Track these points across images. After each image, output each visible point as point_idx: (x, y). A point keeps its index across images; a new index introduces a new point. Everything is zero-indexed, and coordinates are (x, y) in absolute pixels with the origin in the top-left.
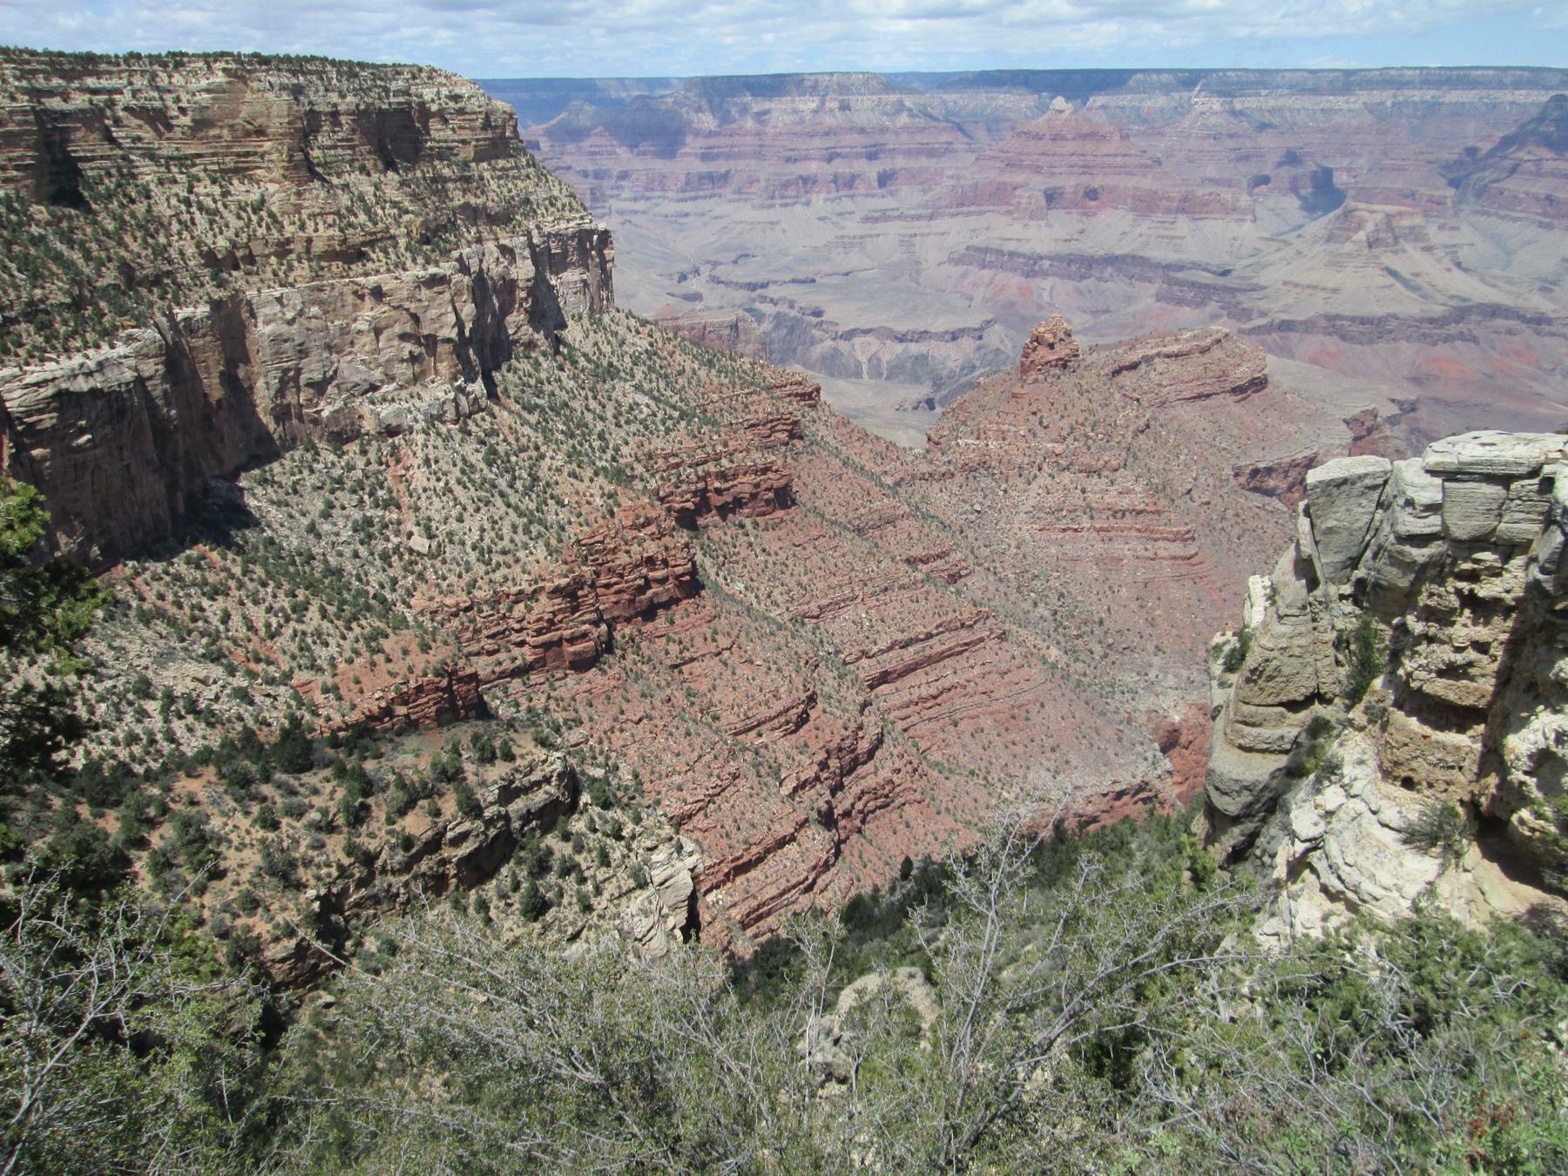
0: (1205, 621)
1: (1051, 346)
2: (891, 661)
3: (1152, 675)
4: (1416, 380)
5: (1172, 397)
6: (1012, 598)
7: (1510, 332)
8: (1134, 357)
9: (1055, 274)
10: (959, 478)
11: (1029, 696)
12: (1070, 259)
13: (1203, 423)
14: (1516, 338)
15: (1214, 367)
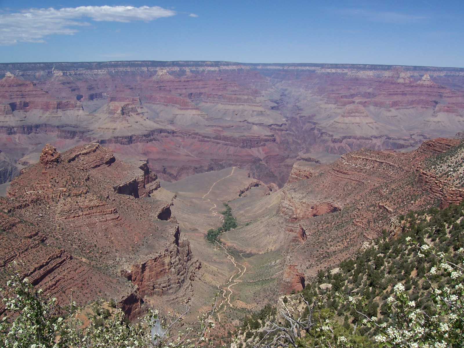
0: (128, 238)
1: (52, 155)
2: (37, 275)
3: (117, 259)
4: (145, 154)
5: (88, 168)
6: (63, 244)
7: (166, 137)
8: (73, 156)
9: (20, 133)
10: (31, 206)
11: (86, 276)
12: (23, 127)
13: (100, 175)
14: (168, 138)
15: (99, 156)
